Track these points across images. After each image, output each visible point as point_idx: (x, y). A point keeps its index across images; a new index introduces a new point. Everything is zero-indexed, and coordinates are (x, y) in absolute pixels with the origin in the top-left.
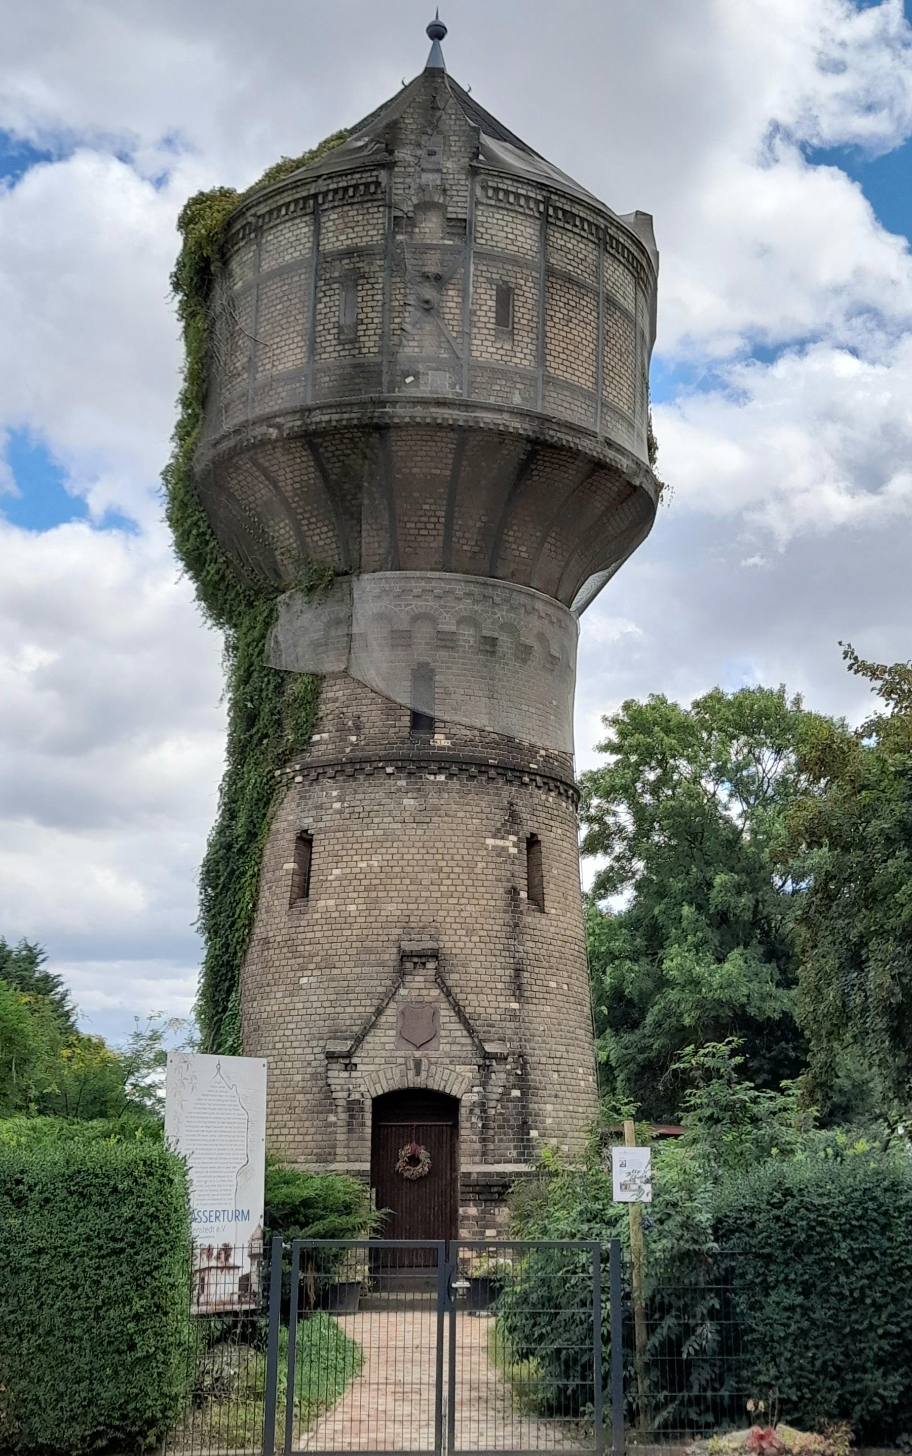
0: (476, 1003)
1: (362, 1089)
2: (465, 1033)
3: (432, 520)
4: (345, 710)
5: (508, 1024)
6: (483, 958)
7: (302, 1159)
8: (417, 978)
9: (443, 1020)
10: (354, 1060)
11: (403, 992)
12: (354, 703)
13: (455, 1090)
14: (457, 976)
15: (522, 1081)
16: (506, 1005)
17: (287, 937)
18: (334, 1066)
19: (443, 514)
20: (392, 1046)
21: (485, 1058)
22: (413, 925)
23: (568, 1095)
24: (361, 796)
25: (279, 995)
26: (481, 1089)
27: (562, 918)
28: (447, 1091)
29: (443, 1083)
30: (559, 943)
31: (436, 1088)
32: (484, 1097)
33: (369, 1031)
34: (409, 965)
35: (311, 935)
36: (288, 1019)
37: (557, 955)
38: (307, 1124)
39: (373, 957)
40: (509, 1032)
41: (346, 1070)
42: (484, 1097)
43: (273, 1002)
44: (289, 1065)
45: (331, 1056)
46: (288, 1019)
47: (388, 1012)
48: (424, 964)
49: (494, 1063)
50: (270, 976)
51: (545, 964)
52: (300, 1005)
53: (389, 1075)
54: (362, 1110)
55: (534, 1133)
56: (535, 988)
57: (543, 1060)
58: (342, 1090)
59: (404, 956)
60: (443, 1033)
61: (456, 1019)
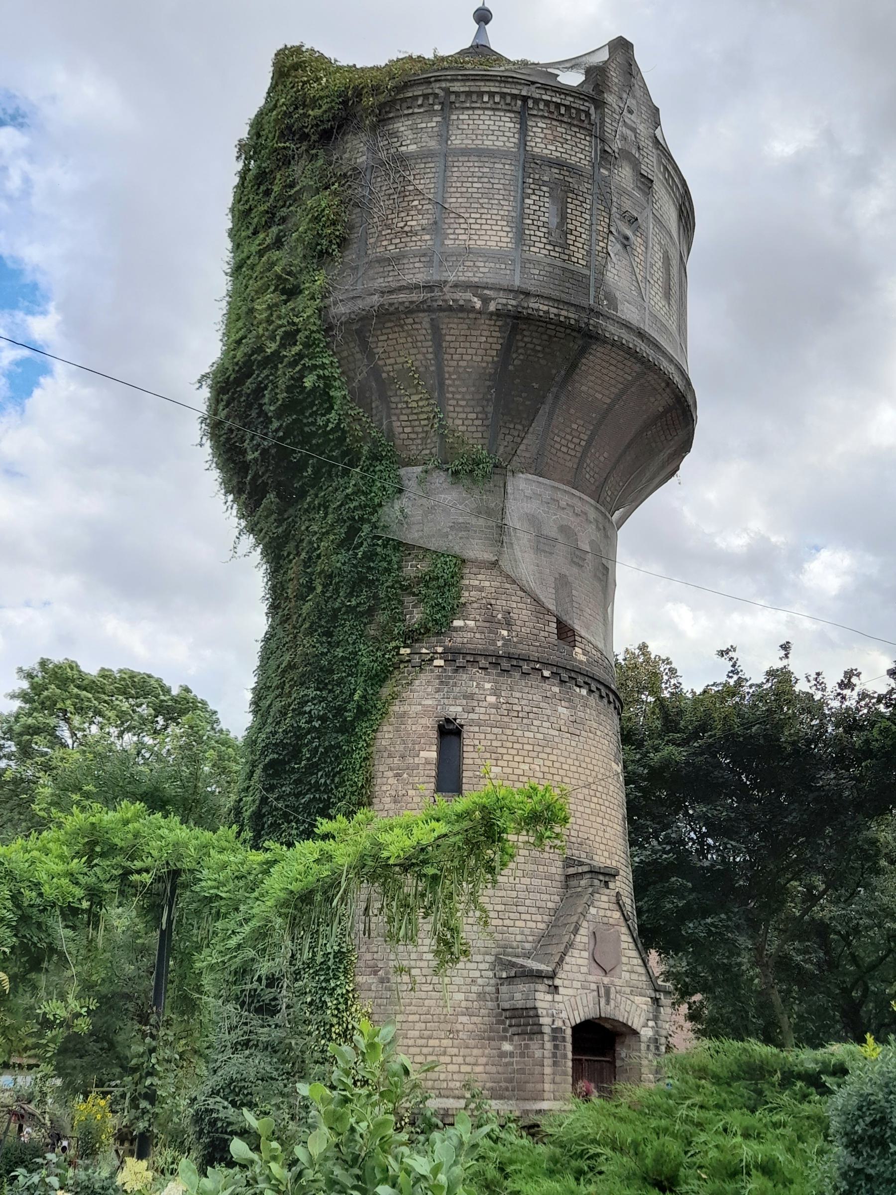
1: (564, 1015)
3: (575, 440)
4: (493, 602)
11: (593, 911)
12: (503, 597)
13: (636, 1024)
19: (586, 438)
21: (656, 990)
24: (518, 695)
38: (475, 1052)
39: (541, 868)
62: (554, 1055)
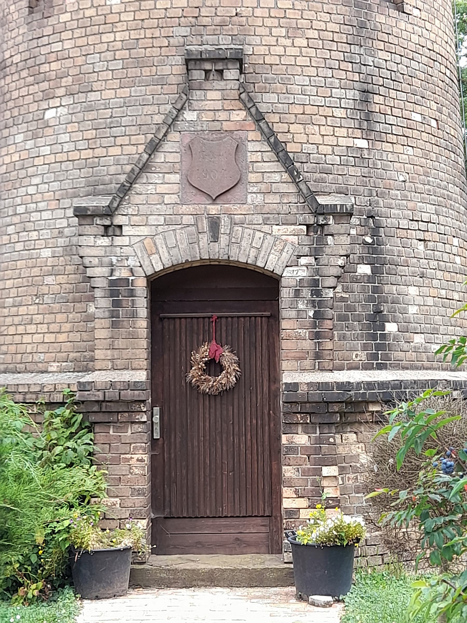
0: (303, 138)
1: (131, 262)
2: (286, 176)
5: (352, 171)
6: (313, 71)
7: (54, 367)
8: (211, 95)
9: (251, 157)
10: (118, 220)
11: (189, 115)
13: (272, 262)
14: (273, 98)
15: (374, 253)
16: (350, 142)
17: (26, 55)
18: (88, 229)
20: (174, 198)
21: (316, 214)
22: (205, 21)
23: (439, 274)
25: (19, 138)
26: (311, 260)
27: (428, 26)
28: (260, 264)
29: (253, 253)
30: (425, 60)
31: (243, 260)
32: (317, 272)
33: (137, 177)
34: (198, 75)
35: (57, 47)
36: (31, 171)
37: (422, 76)
38: (60, 317)
39: (146, 72)
40: (352, 181)
41: (105, 234)
42: (317, 272)
43: (12, 149)
44: (34, 235)
45: (82, 214)
46: (31, 171)
47: (167, 146)
48: (221, 72)
49: (331, 222)
50: (8, 114)
51: (405, 86)
52: (46, 150)
53: (171, 242)
54: (132, 293)
55: (391, 328)
56: (391, 120)
57: (404, 223)
58: (101, 265)
59: (190, 62)
60: (252, 177)
61: (271, 155)
62: (113, 315)
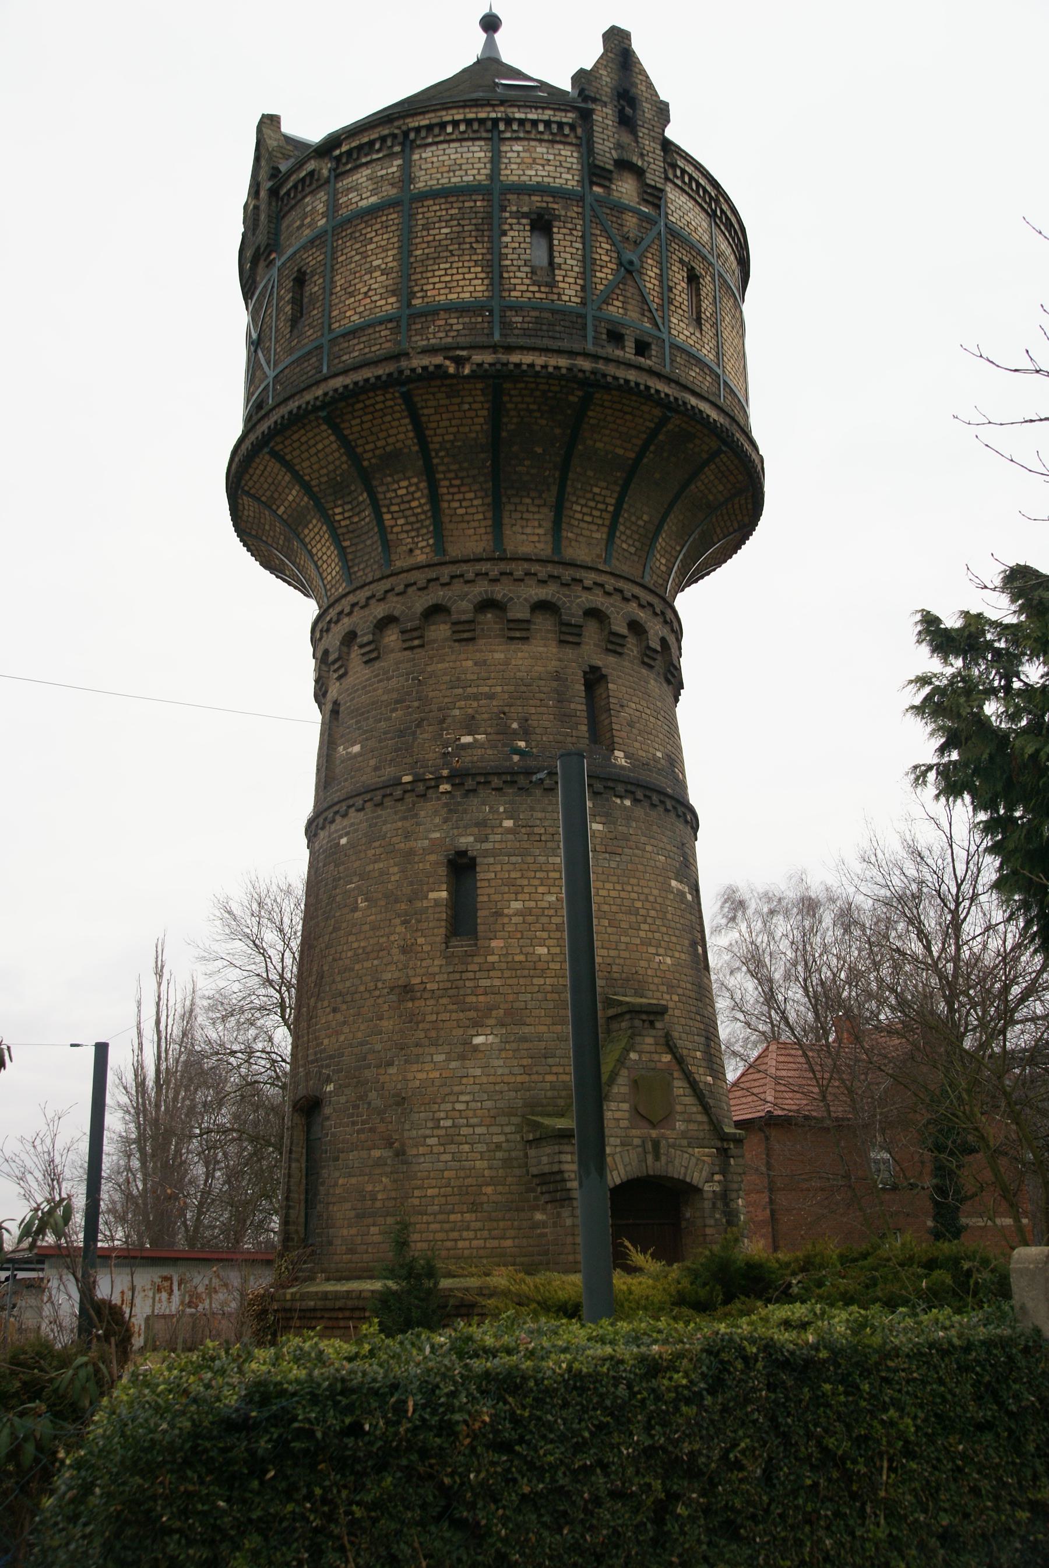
3: (600, 506)
4: (506, 709)
11: (633, 1056)
12: (518, 702)
13: (696, 1177)
19: (613, 501)
22: (616, 976)
24: (540, 815)
29: (683, 1170)
31: (676, 1176)
44: (466, 1148)
48: (652, 1023)
53: (627, 1160)
61: (688, 1091)
